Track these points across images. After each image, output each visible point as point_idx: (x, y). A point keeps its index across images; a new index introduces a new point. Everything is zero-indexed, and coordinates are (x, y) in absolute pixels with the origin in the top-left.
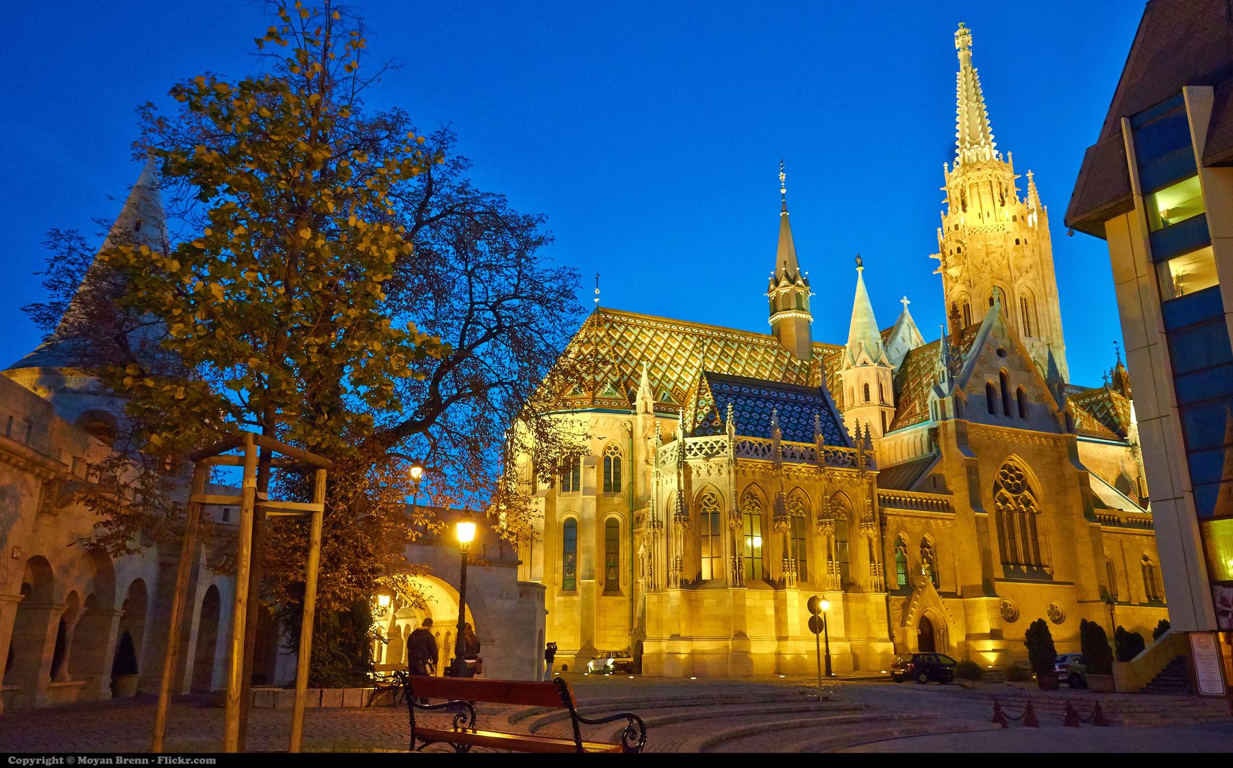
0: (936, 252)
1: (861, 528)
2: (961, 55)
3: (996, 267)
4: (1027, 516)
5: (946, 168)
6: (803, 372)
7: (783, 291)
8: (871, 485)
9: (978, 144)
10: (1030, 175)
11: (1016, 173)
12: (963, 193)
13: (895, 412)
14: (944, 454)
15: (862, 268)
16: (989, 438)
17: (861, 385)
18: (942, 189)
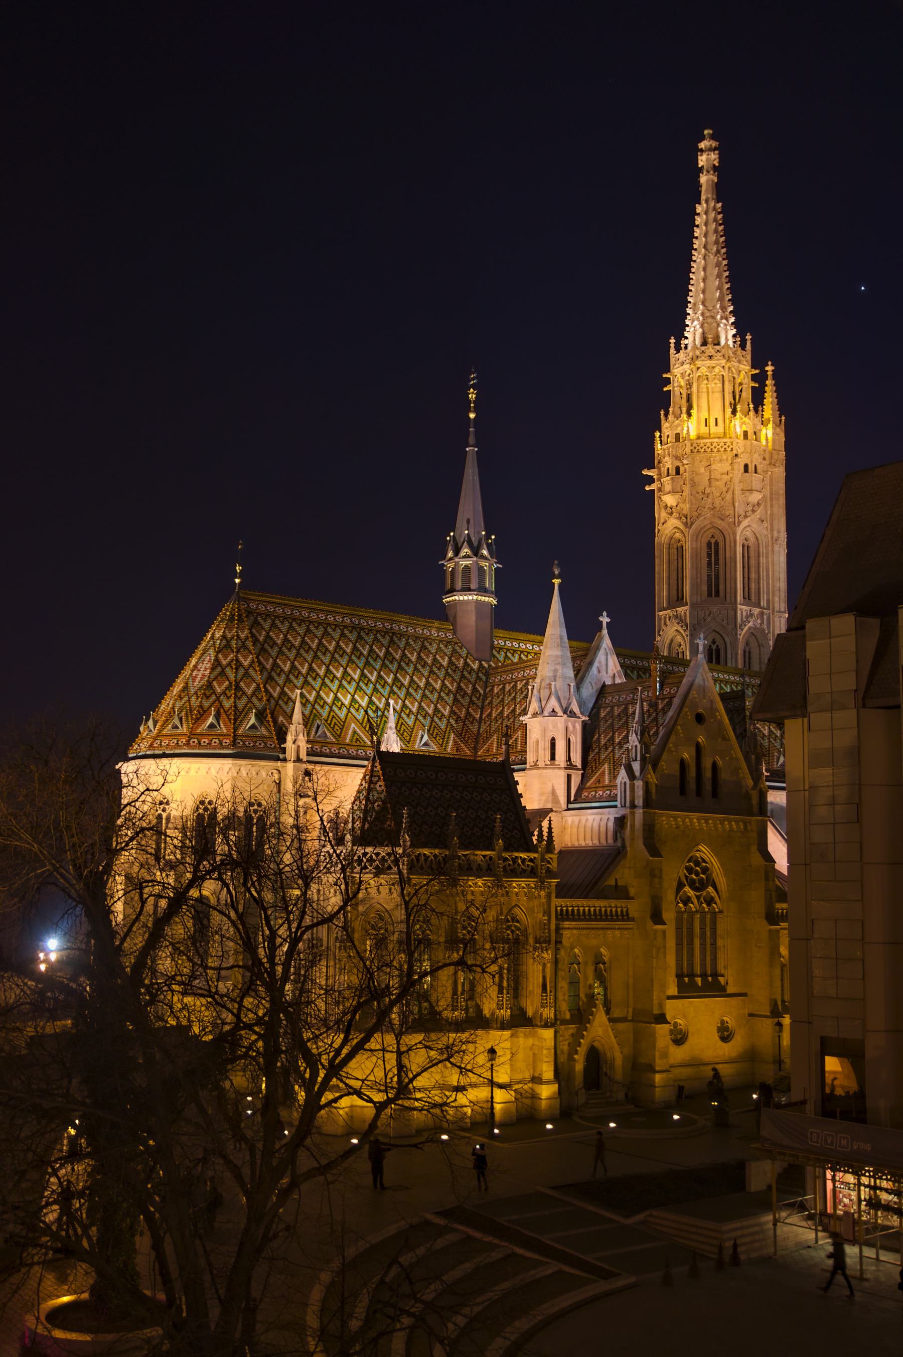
0: (652, 467)
1: (535, 949)
2: (703, 179)
3: (718, 502)
4: (708, 917)
5: (672, 345)
6: (481, 679)
7: (464, 563)
8: (549, 896)
10: (769, 368)
11: (753, 366)
12: (689, 385)
13: (583, 775)
14: (628, 849)
15: (559, 580)
16: (678, 827)
18: (664, 376)
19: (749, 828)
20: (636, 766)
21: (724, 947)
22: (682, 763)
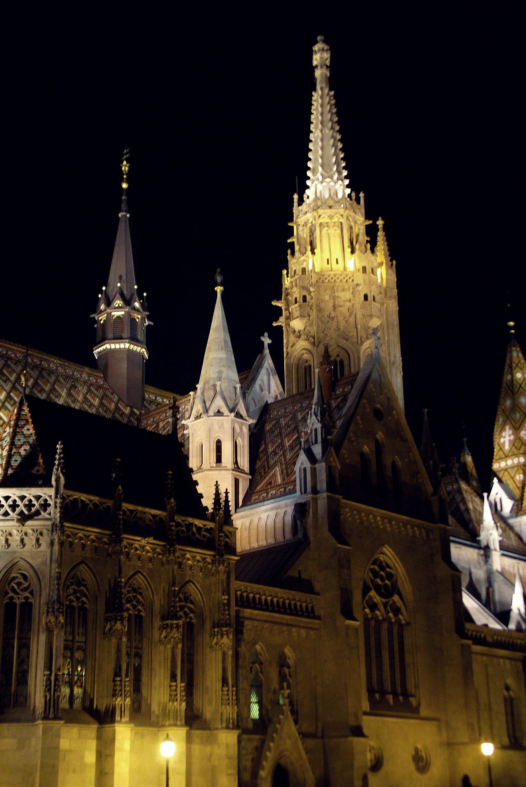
0: (279, 299)
1: (212, 635)
2: (318, 73)
3: (342, 324)
4: (396, 628)
7: (116, 314)
8: (228, 574)
9: (331, 177)
10: (380, 223)
11: (367, 217)
12: (312, 232)
13: (251, 481)
14: (312, 538)
16: (361, 523)
17: (212, 441)
19: (431, 536)
20: (317, 450)
21: (413, 663)
22: (363, 455)
